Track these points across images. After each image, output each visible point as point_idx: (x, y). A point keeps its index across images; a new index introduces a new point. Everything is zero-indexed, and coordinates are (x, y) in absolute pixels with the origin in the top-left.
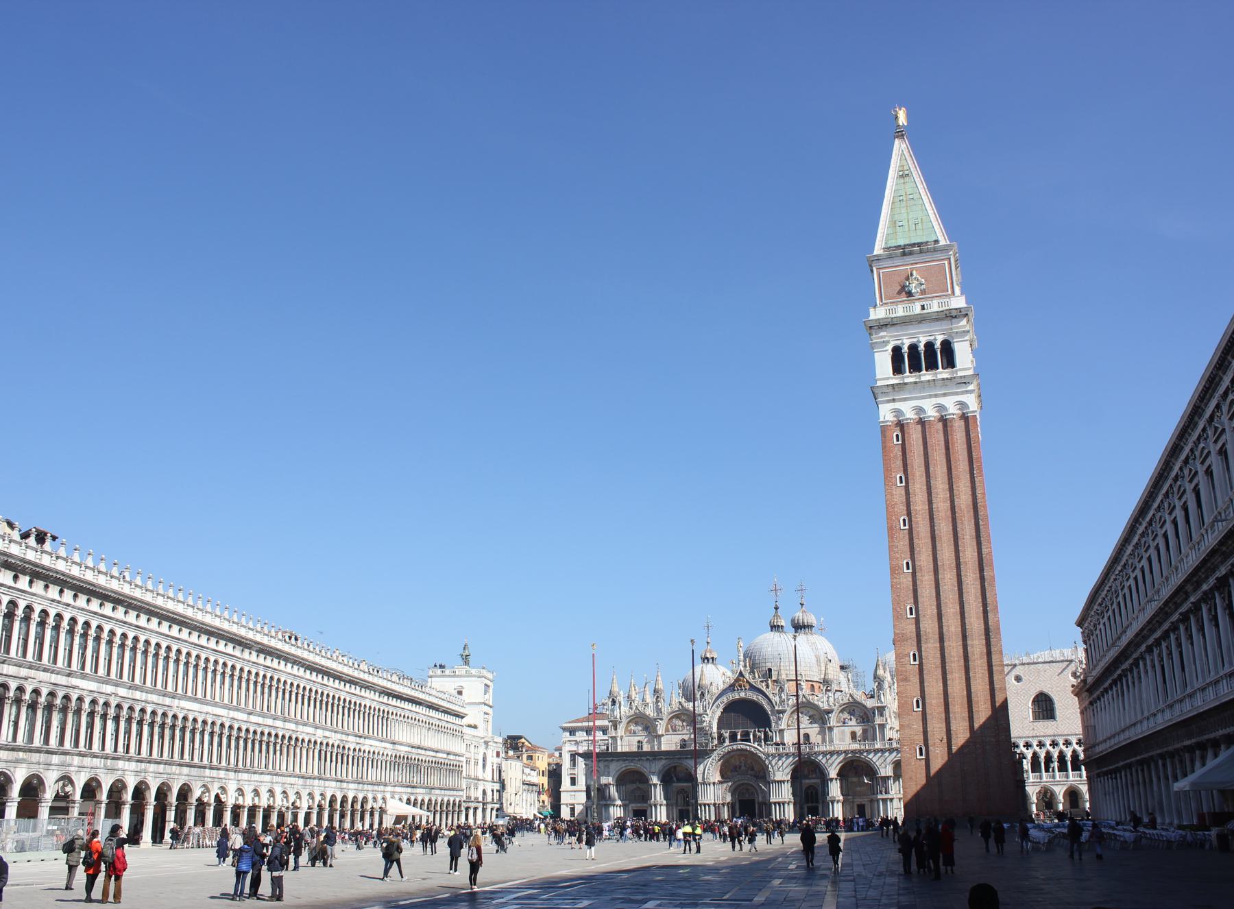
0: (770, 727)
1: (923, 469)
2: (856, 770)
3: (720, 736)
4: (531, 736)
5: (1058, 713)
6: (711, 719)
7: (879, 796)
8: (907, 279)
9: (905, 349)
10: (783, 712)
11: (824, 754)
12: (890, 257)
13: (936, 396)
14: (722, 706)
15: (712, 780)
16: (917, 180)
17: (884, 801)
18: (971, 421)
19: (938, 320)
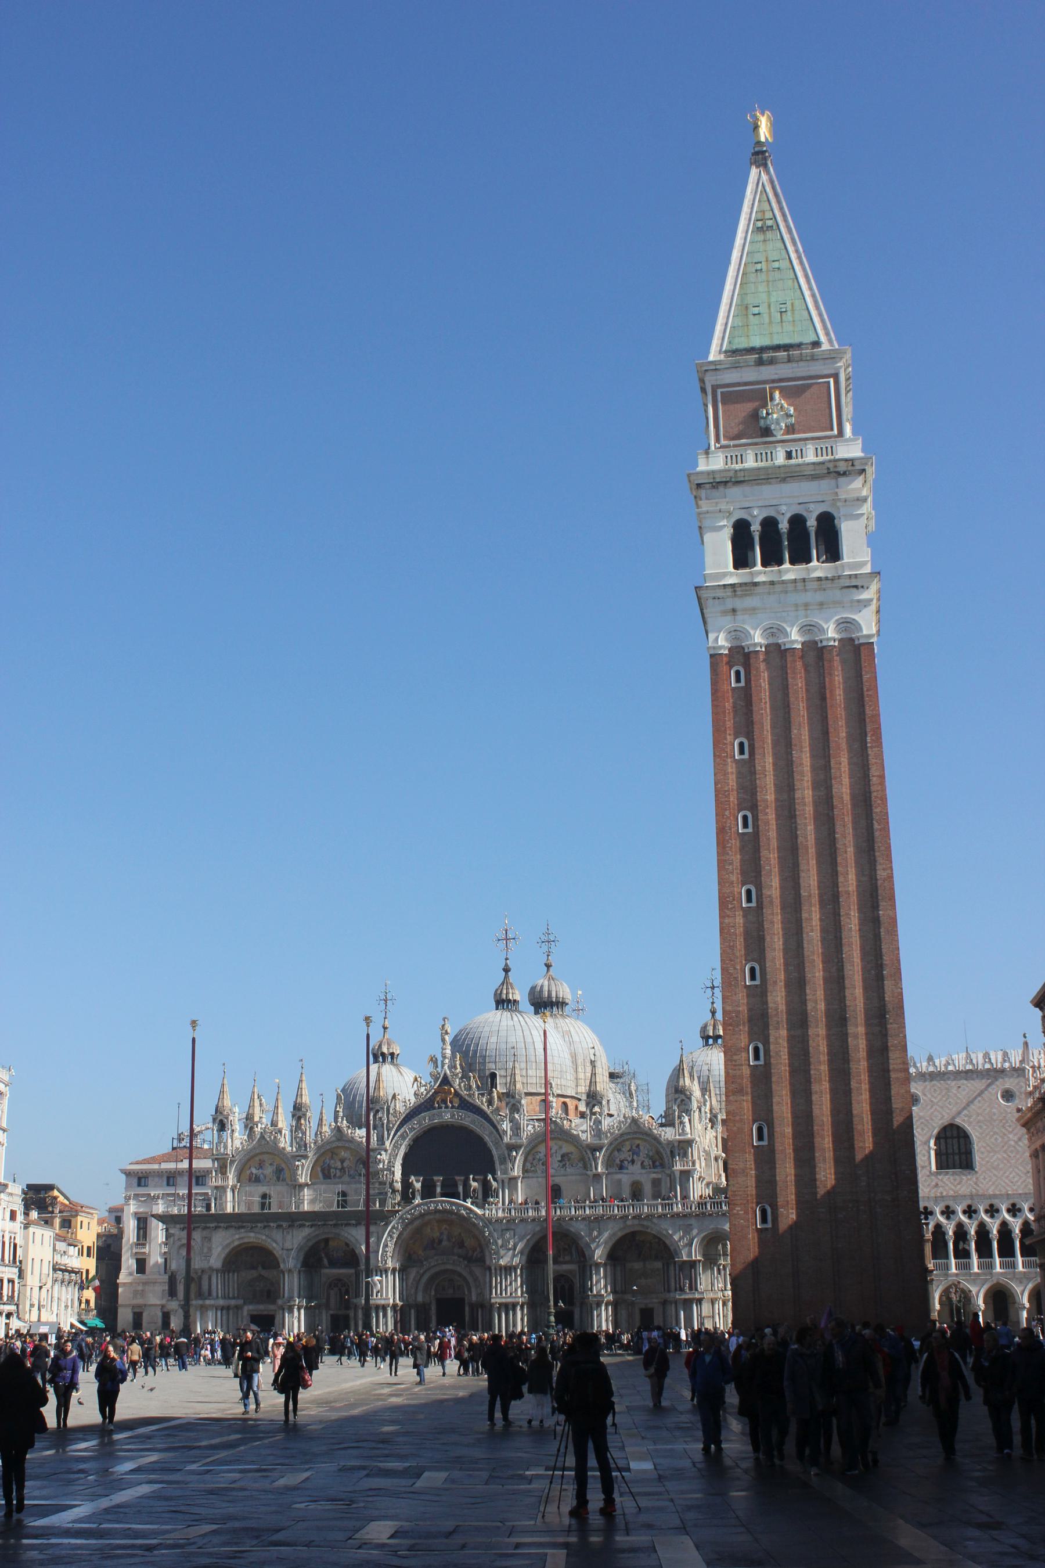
0: (494, 1174)
3: (406, 1184)
4: (69, 1188)
5: (977, 1158)
9: (756, 528)
12: (735, 367)
19: (814, 477)
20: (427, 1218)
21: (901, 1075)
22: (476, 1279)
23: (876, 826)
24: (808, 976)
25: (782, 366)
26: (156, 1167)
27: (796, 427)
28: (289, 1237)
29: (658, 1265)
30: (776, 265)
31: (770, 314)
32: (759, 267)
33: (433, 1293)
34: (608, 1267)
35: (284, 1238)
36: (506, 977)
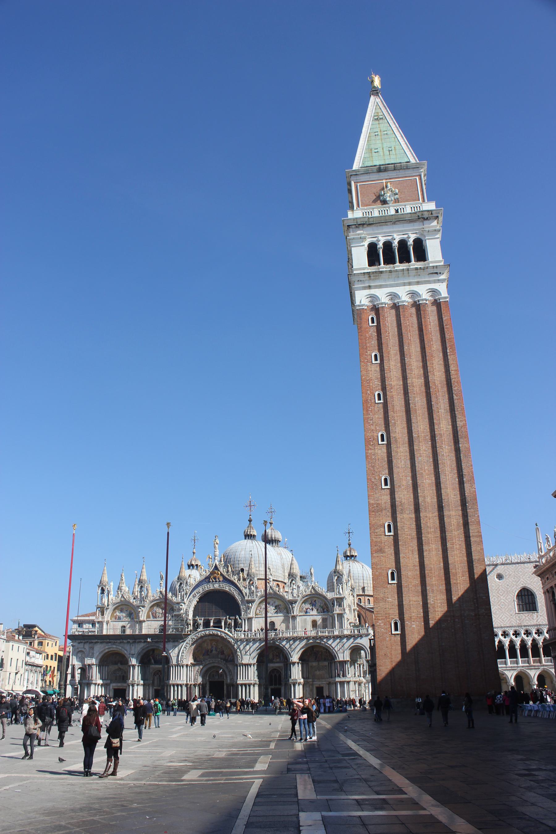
0: (240, 615)
1: (397, 348)
2: (318, 656)
3: (195, 621)
6: (188, 607)
7: (338, 679)
8: (383, 189)
10: (252, 602)
11: (288, 639)
13: (410, 284)
14: (198, 596)
15: (185, 663)
16: (391, 122)
17: (342, 683)
18: (443, 306)
19: (411, 221)
20: (204, 638)
21: (478, 539)
22: (230, 671)
23: (455, 397)
24: (419, 482)
25: (391, 172)
26: (87, 618)
27: (400, 199)
28: (133, 648)
29: (326, 663)
30: (385, 132)
31: (383, 152)
32: (377, 134)
33: (207, 678)
34: (300, 665)
35: (131, 648)
36: (250, 524)
